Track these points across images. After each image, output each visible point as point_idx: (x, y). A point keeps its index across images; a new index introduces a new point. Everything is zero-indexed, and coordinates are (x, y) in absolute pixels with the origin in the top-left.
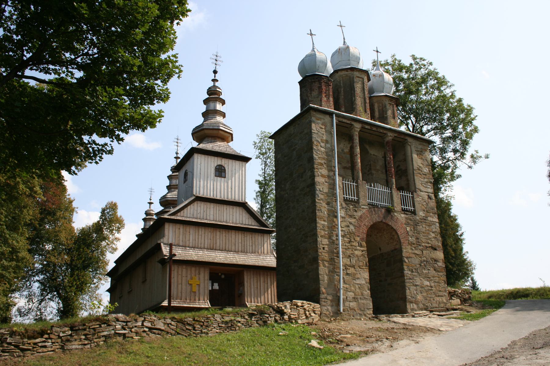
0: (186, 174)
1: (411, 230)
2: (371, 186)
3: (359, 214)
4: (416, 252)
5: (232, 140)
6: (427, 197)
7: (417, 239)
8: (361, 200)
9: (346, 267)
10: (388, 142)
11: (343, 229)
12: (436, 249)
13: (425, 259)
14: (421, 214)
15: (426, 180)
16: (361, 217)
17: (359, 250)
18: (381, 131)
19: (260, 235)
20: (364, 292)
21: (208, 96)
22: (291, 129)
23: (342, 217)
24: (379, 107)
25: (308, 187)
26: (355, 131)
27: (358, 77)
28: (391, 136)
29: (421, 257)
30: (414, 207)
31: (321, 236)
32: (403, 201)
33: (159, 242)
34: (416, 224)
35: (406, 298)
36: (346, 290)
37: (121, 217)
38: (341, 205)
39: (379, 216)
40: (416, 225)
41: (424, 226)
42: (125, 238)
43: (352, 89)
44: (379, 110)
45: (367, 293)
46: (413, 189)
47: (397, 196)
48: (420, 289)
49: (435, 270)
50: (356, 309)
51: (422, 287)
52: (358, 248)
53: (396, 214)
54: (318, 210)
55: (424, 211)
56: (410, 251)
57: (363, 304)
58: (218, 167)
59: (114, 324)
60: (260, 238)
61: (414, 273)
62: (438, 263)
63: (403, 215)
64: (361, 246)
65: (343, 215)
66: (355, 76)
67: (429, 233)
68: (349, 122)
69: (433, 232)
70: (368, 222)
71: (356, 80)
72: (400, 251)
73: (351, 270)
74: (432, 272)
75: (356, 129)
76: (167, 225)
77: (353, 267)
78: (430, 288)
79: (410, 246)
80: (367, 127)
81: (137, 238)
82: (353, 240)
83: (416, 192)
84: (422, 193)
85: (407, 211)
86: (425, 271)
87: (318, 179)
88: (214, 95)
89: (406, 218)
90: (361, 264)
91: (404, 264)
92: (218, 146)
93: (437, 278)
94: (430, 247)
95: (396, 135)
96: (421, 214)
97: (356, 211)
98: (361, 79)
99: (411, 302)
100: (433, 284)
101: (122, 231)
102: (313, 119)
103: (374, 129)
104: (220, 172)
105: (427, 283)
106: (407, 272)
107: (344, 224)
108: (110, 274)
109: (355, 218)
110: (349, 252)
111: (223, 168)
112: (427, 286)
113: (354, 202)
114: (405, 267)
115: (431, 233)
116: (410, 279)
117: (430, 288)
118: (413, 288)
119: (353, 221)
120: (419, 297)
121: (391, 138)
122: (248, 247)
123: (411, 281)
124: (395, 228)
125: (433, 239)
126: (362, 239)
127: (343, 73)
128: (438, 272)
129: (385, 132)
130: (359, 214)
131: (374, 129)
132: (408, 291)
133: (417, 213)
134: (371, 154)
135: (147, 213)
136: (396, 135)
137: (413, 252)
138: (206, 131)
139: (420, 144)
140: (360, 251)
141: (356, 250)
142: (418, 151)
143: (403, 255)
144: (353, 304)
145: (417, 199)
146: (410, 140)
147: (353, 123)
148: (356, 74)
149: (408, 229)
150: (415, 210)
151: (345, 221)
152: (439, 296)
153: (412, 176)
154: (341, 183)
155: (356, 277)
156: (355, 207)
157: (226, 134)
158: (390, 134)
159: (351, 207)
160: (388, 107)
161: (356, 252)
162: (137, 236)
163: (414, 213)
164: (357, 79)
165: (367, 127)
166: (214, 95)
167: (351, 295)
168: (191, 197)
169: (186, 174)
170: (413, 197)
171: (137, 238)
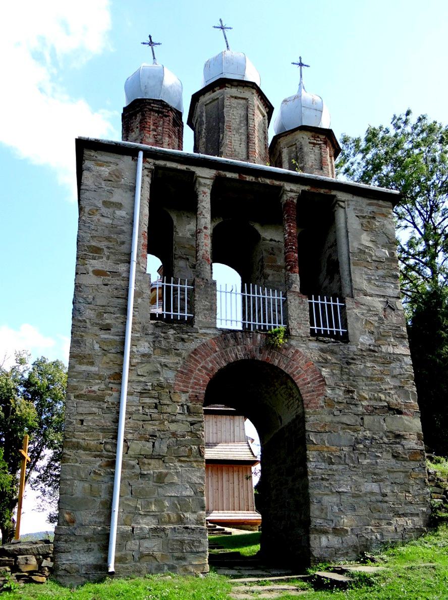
4: (345, 419)
7: (348, 392)
10: (288, 204)
12: (400, 412)
14: (364, 340)
15: (381, 272)
16: (195, 352)
18: (268, 181)
19: (228, 417)
20: (187, 515)
26: (200, 184)
28: (291, 191)
30: (345, 326)
32: (314, 315)
35: (309, 522)
41: (369, 365)
43: (220, 118)
46: (347, 290)
48: (351, 500)
49: (394, 457)
52: (179, 417)
53: (293, 343)
55: (372, 333)
56: (328, 419)
60: (228, 422)
61: (334, 467)
62: (404, 442)
63: (314, 345)
67: (381, 379)
68: (184, 167)
69: (394, 377)
73: (154, 468)
74: (385, 460)
75: (202, 181)
77: (160, 457)
78: (380, 498)
79: (327, 409)
80: (229, 175)
83: (352, 297)
84: (368, 298)
86: (365, 462)
93: (403, 475)
94: (384, 407)
95: (306, 188)
96: (364, 340)
97: (183, 340)
99: (325, 532)
100: (387, 490)
103: (249, 178)
105: (375, 487)
106: (314, 464)
109: (179, 355)
112: (372, 493)
115: (388, 379)
116: (323, 479)
117: (380, 498)
119: (170, 360)
120: (346, 521)
121: (293, 194)
122: (211, 434)
123: (325, 483)
125: (392, 392)
127: (208, 97)
128: (405, 460)
129: (277, 183)
131: (249, 178)
133: (351, 338)
136: (306, 188)
137: (336, 419)
139: (370, 205)
141: (173, 421)
142: (364, 217)
146: (341, 196)
147: (193, 168)
149: (325, 372)
150: (346, 335)
151: (148, 362)
152: (404, 515)
155: (167, 480)
158: (288, 186)
161: (173, 427)
165: (229, 175)
170: (343, 308)
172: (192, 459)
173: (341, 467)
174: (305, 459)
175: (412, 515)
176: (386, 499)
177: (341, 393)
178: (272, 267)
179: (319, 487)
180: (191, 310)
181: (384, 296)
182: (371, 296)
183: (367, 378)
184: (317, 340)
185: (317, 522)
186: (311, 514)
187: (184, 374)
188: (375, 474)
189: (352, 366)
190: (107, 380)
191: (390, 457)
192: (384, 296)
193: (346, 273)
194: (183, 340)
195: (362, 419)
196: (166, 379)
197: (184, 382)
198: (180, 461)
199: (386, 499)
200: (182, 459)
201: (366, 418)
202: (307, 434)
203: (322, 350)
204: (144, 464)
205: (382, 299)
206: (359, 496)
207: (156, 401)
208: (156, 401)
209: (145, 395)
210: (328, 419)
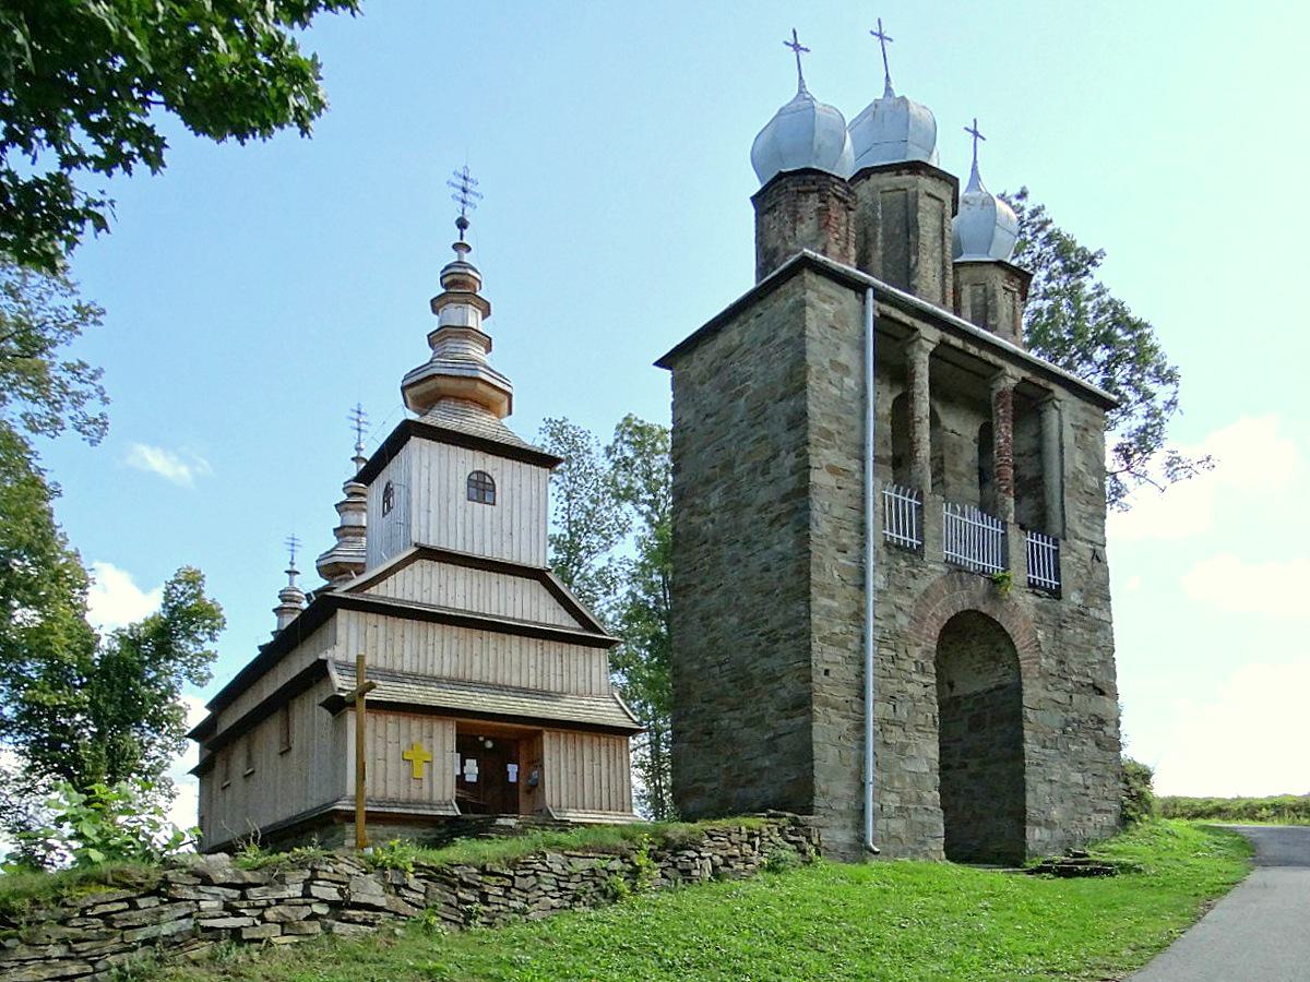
0: (388, 492)
1: (1047, 639)
2: (954, 509)
3: (921, 585)
5: (510, 413)
6: (1090, 554)
7: (1061, 662)
8: (928, 549)
9: (884, 724)
11: (880, 623)
12: (1102, 693)
13: (1075, 715)
14: (1075, 598)
16: (926, 593)
17: (918, 683)
20: (925, 794)
21: (443, 291)
22: (733, 335)
23: (879, 591)
24: (973, 295)
25: (785, 498)
27: (930, 195)
29: (1066, 711)
30: (1058, 578)
31: (823, 639)
33: (322, 657)
34: (1060, 625)
35: (1025, 812)
36: (881, 788)
37: (213, 601)
38: (877, 554)
39: (970, 595)
40: (1061, 627)
41: (1079, 630)
42: (234, 648)
44: (973, 306)
45: (933, 796)
46: (1057, 529)
47: (1019, 543)
49: (1098, 745)
50: (903, 836)
51: (1064, 786)
52: (915, 676)
54: (818, 565)
56: (1043, 694)
57: (922, 824)
58: (475, 477)
59: (191, 894)
61: (1047, 751)
63: (1030, 598)
64: (923, 670)
65: (882, 586)
66: (921, 191)
67: (1089, 650)
69: (1099, 648)
70: (942, 612)
71: (923, 202)
72: (1018, 690)
73: (896, 736)
76: (342, 614)
77: (902, 725)
78: (1083, 791)
81: (259, 653)
82: (902, 655)
83: (1065, 539)
85: (1039, 587)
86: (1073, 748)
87: (818, 477)
88: (458, 286)
89: (1037, 605)
90: (921, 720)
91: (1026, 725)
92: (479, 423)
94: (1089, 684)
97: (914, 576)
98: (936, 203)
99: (1038, 824)
101: (221, 635)
102: (810, 296)
104: (481, 488)
105: (1077, 777)
106: (1030, 747)
107: (883, 610)
108: (197, 734)
109: (911, 596)
110: (892, 687)
111: (488, 480)
113: (910, 550)
114: (1027, 734)
115: (1094, 651)
116: (1038, 765)
118: (1043, 788)
120: (1056, 814)
123: (1040, 769)
124: (1008, 630)
125: (1097, 667)
126: (926, 653)
130: (921, 585)
132: (1029, 796)
134: (946, 430)
135: (283, 597)
137: (1049, 695)
138: (440, 382)
140: (921, 687)
141: (908, 682)
143: (1024, 703)
144: (897, 825)
145: (1067, 559)
148: (926, 183)
149: (1040, 635)
150: (1059, 587)
152: (1100, 811)
153: (1057, 495)
154: (878, 495)
155: (908, 752)
156: (913, 565)
157: (495, 393)
159: (903, 563)
160: (1000, 294)
161: (910, 688)
162: (260, 648)
163: (1056, 594)
164: (928, 200)
166: (458, 286)
167: (892, 800)
168: (405, 548)
169: (388, 492)
170: (1056, 552)
171: (259, 653)
172: (928, 730)
173: (1053, 752)
174: (1021, 739)
175: (1106, 811)
176: (1088, 792)
177: (1054, 663)
178: (953, 472)
179: (1034, 773)
180: (920, 536)
181: (1092, 542)
182: (1081, 539)
183: (1076, 646)
184: (1033, 593)
185: (1031, 812)
186: (1027, 804)
187: (918, 620)
188: (1080, 763)
189: (1064, 631)
190: (848, 622)
191: (1094, 745)
192: (1092, 542)
193: (1057, 504)
194: (914, 576)
195: (1071, 697)
196: (901, 626)
197: (916, 631)
198: (918, 731)
199: (1088, 792)
200: (921, 728)
201: (1074, 696)
202: (1024, 709)
203: (1037, 605)
204: (887, 730)
205: (1090, 546)
206: (1066, 787)
207: (894, 654)
208: (894, 654)
209: (884, 645)
210: (1043, 694)
